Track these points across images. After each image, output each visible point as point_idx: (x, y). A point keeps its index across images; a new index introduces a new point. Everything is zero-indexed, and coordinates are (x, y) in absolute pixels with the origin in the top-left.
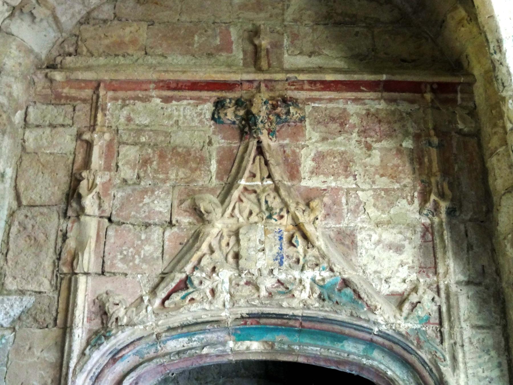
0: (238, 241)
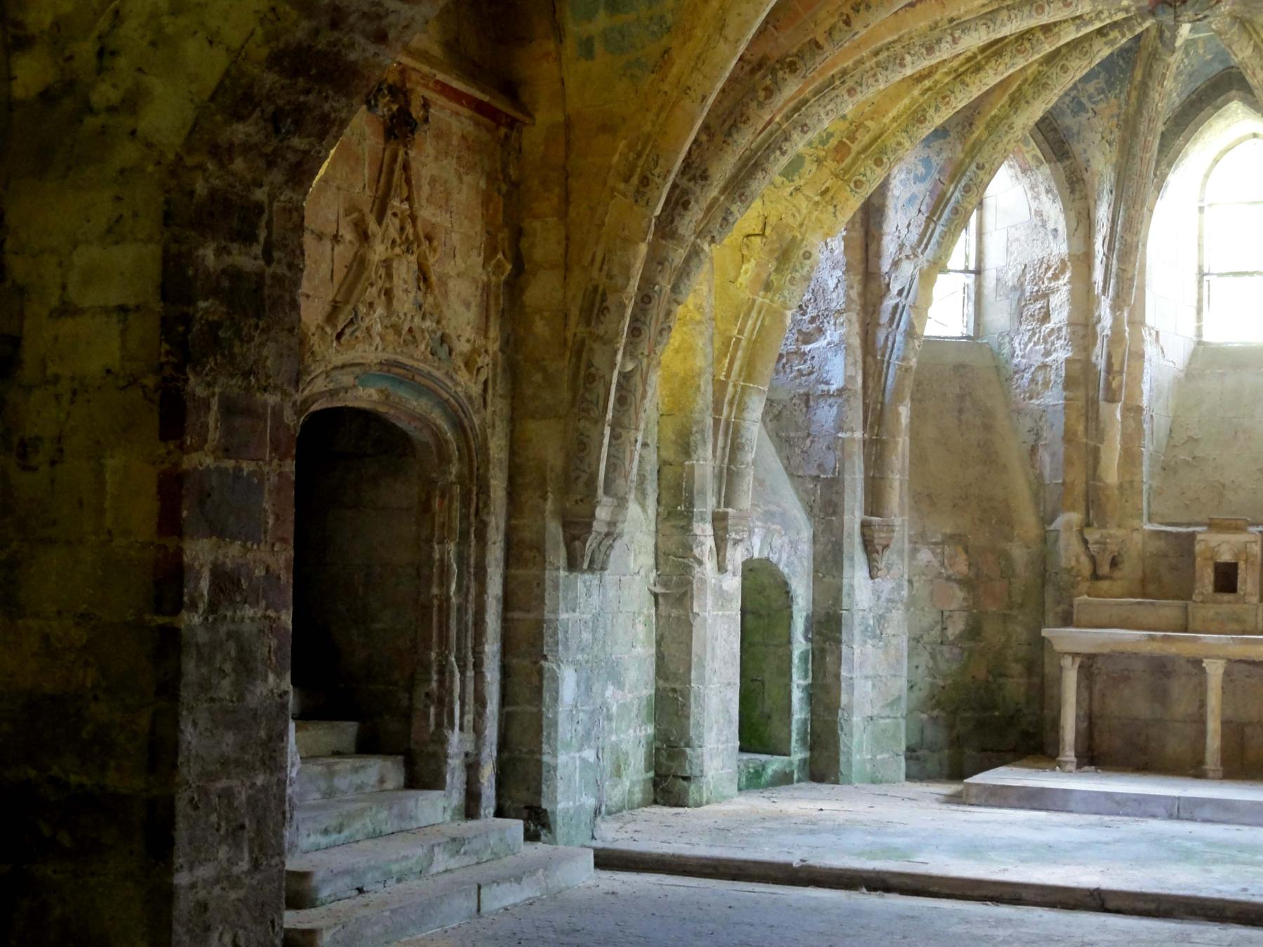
0: (389, 276)
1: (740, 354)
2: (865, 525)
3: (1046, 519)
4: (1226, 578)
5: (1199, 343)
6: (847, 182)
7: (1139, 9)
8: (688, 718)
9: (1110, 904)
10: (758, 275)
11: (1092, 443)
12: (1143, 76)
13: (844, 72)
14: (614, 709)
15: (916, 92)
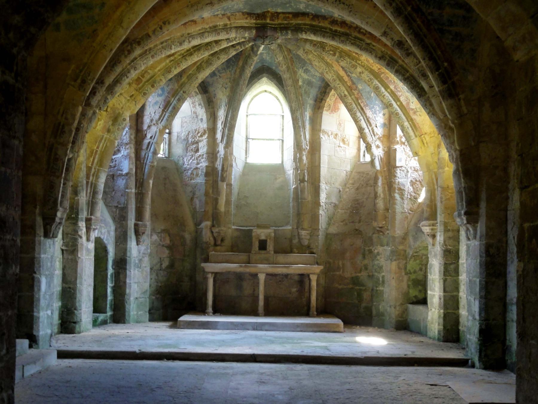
1: (97, 156)
2: (136, 225)
3: (197, 224)
4: (263, 245)
5: (246, 163)
7: (249, 38)
8: (75, 298)
9: (258, 360)
10: (105, 126)
11: (215, 196)
12: (243, 64)
13: (150, 49)
15: (168, 61)
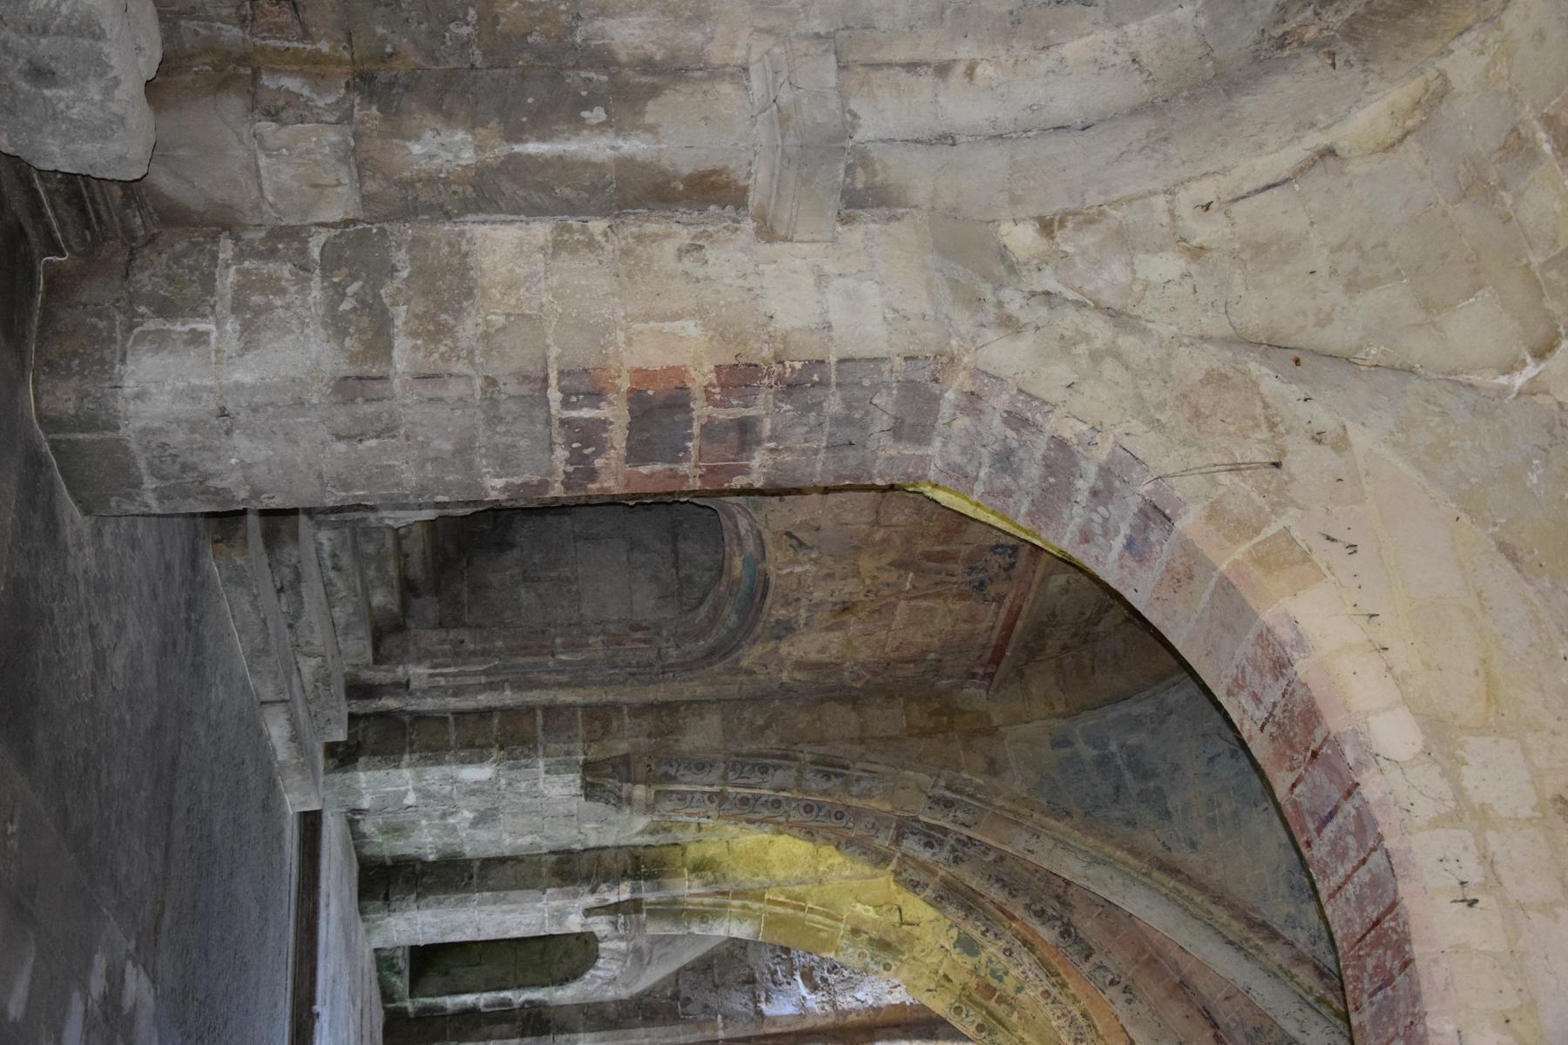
1: (790, 911)
6: (959, 999)
10: (865, 922)
13: (1064, 985)
14: (451, 821)
